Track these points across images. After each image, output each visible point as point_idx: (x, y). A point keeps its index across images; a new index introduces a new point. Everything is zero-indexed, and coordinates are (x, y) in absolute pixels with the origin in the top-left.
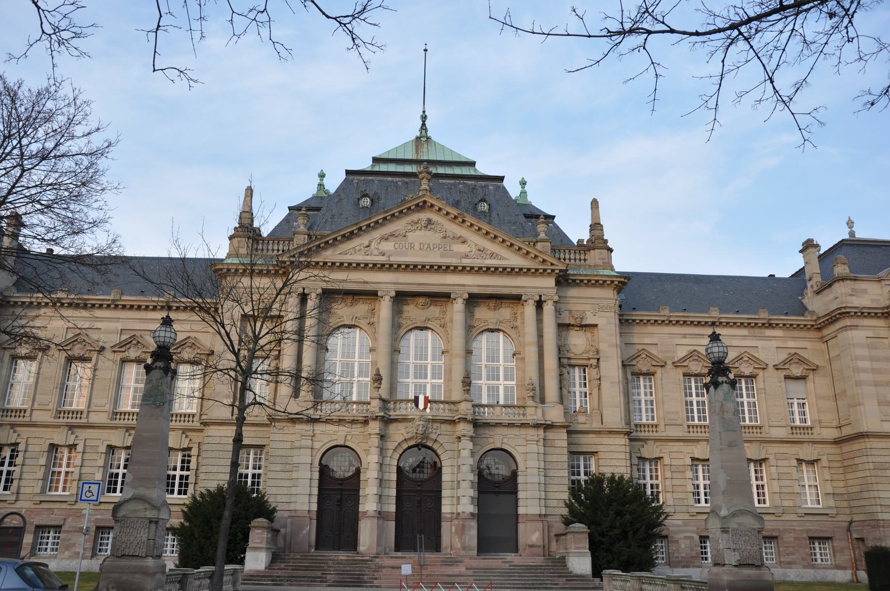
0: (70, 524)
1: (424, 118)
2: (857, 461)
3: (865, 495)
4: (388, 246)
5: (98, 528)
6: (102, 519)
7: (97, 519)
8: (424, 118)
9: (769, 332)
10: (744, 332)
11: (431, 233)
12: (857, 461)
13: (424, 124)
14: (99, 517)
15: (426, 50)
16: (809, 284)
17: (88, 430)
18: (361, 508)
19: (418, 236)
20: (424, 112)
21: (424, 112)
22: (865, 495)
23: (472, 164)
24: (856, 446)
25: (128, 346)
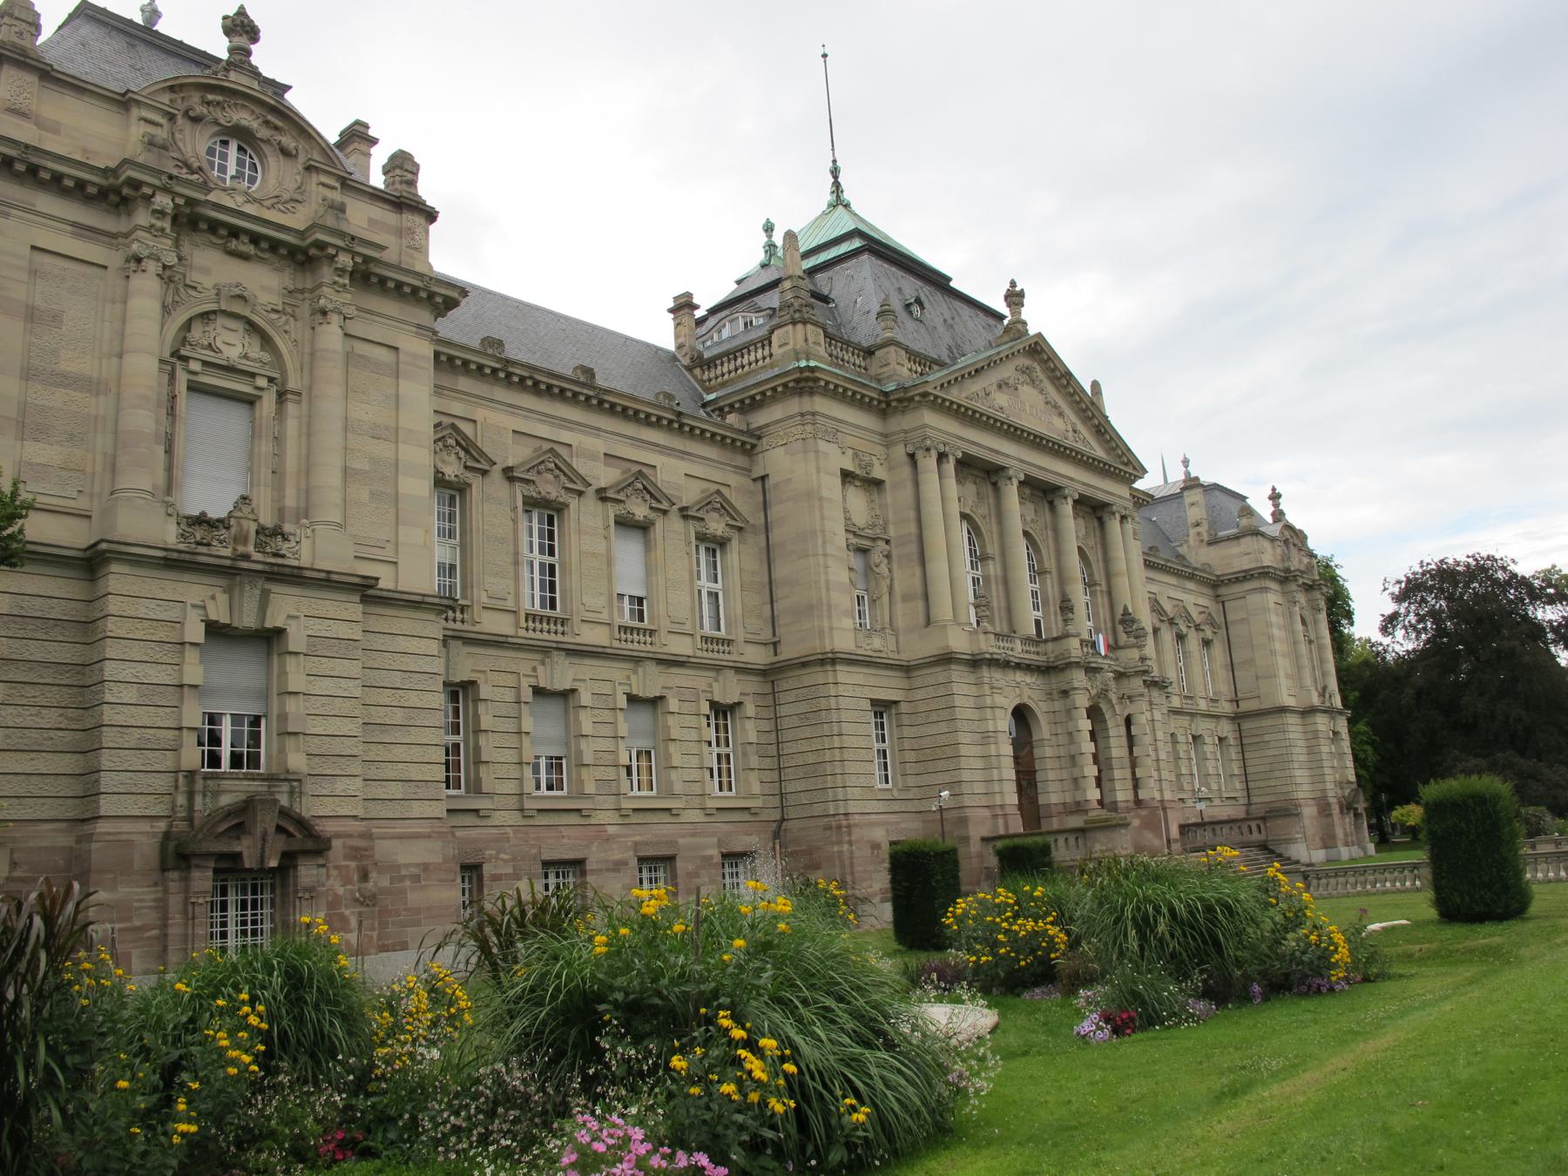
0: (595, 856)
1: (835, 172)
2: (1266, 738)
3: (1277, 774)
4: (1001, 399)
5: (641, 860)
6: (646, 843)
7: (636, 844)
8: (835, 172)
9: (1191, 585)
10: (1173, 580)
11: (1035, 392)
12: (1266, 738)
13: (836, 177)
14: (638, 838)
15: (825, 56)
16: (1193, 531)
17: (588, 661)
18: (1042, 800)
19: (1026, 391)
20: (834, 161)
21: (834, 161)
22: (1277, 774)
23: (949, 279)
24: (1266, 722)
25: (629, 491)
